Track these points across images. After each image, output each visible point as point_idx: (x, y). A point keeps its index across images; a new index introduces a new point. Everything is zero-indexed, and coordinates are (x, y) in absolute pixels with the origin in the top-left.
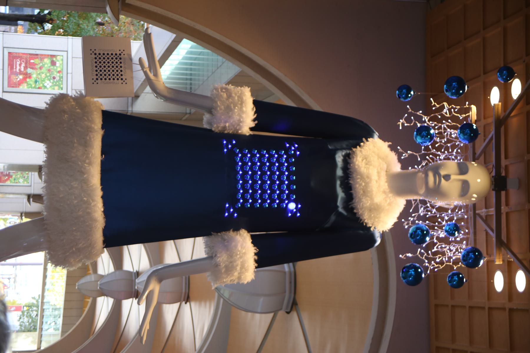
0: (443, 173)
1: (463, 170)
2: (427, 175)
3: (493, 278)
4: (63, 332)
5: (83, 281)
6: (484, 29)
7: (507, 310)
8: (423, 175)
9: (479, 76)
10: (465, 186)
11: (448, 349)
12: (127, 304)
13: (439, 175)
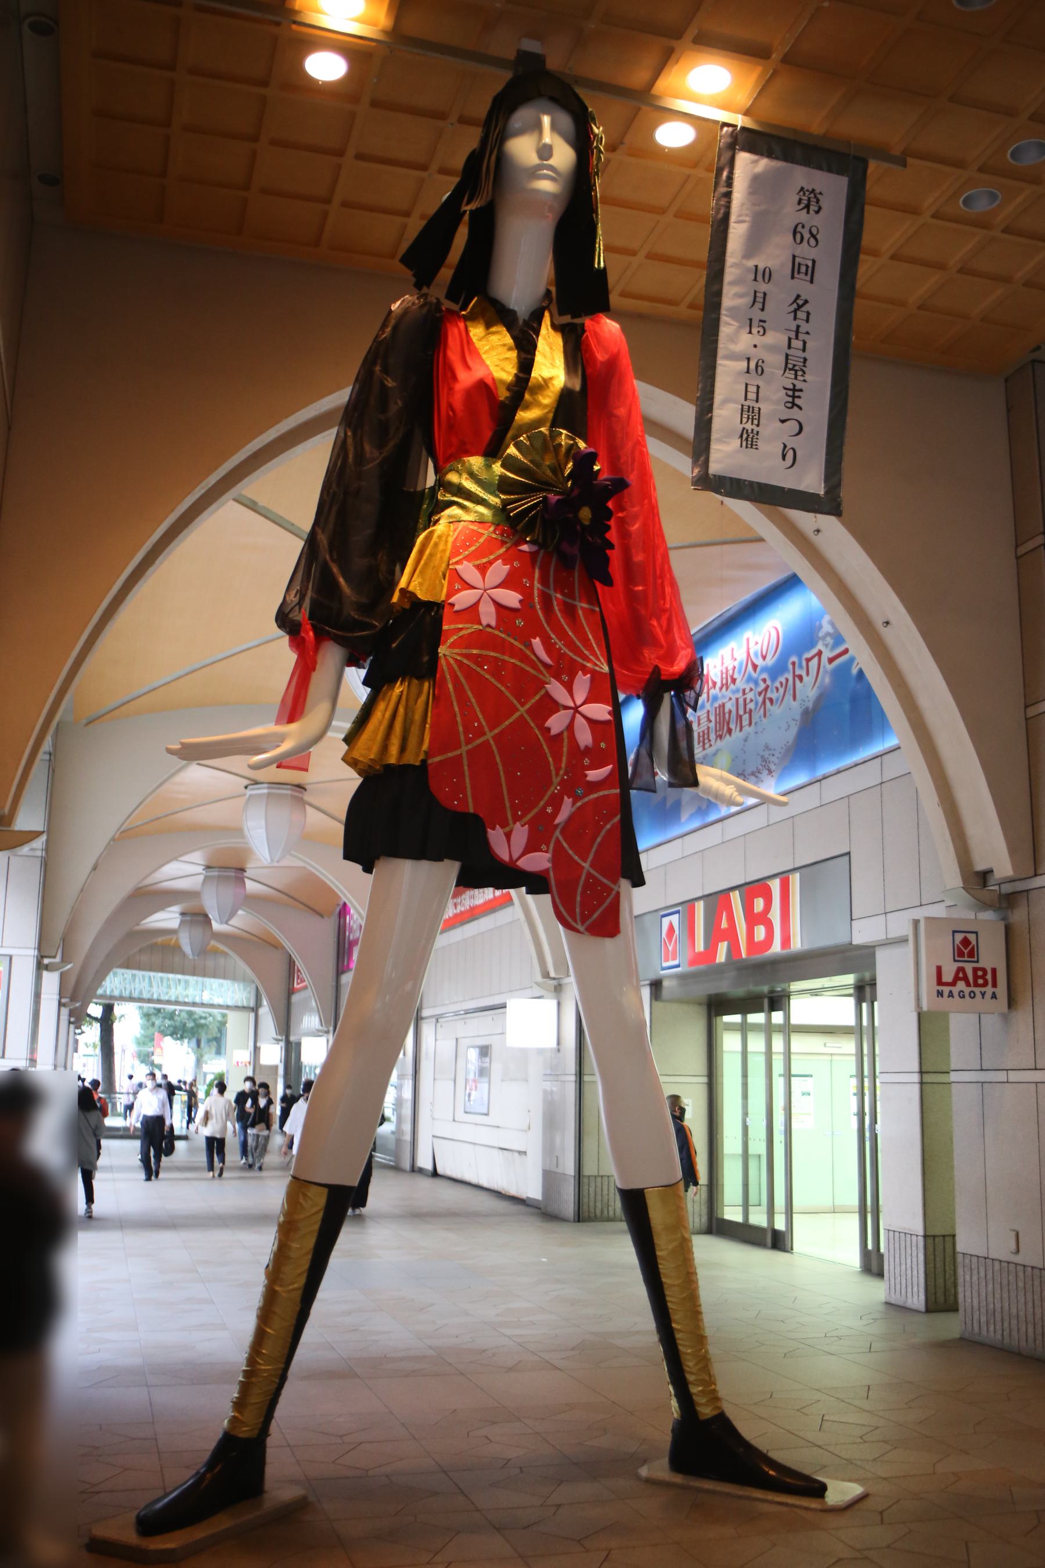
5: (187, 949)
12: (250, 885)
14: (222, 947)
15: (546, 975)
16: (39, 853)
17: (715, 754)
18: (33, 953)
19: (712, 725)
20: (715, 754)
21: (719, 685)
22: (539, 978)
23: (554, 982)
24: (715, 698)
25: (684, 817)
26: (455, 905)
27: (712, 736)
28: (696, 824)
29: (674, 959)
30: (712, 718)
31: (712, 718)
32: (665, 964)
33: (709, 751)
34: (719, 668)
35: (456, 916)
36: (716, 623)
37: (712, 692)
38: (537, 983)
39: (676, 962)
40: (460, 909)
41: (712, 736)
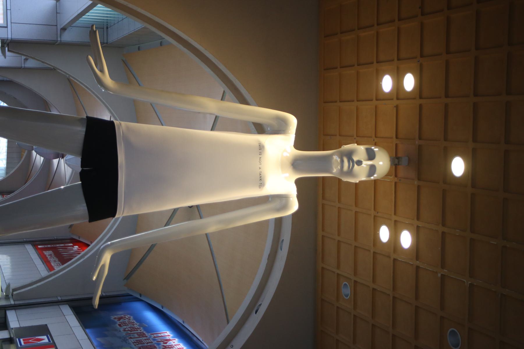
0: (355, 159)
1: (371, 156)
2: (342, 161)
3: (379, 231)
4: (7, 173)
6: (378, 24)
7: (392, 259)
8: (339, 160)
9: (372, 63)
10: (372, 169)
11: (334, 272)
12: (55, 161)
13: (353, 161)
14: (23, 159)
15: (14, 290)
16: (59, 39)
17: (131, 347)
18: (10, 37)
19: (146, 345)
20: (131, 347)
21: (165, 345)
22: (12, 286)
23: (10, 295)
24: (159, 344)
25: (98, 339)
26: (51, 255)
27: (140, 345)
28: (95, 343)
29: (24, 343)
30: (149, 344)
31: (149, 344)
32: (22, 340)
33: (133, 346)
34: (173, 344)
35: (45, 255)
36: (195, 339)
37: (162, 343)
38: (8, 286)
39: (23, 344)
40: (49, 257)
41: (140, 345)
